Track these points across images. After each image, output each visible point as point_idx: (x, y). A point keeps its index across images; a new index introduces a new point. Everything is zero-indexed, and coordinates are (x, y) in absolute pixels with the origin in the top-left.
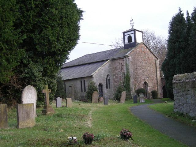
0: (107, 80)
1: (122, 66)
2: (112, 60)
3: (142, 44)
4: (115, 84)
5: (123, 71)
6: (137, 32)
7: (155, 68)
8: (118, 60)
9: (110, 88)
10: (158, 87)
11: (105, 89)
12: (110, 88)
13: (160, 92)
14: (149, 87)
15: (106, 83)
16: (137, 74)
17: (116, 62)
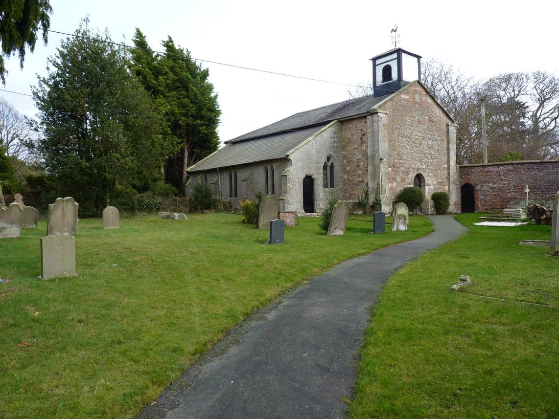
0: (325, 167)
1: (363, 135)
2: (342, 122)
3: (417, 84)
4: (346, 177)
5: (364, 146)
6: (404, 55)
7: (446, 142)
8: (355, 122)
9: (332, 186)
10: (449, 186)
12: (332, 186)
13: (454, 198)
14: (427, 187)
17: (350, 125)
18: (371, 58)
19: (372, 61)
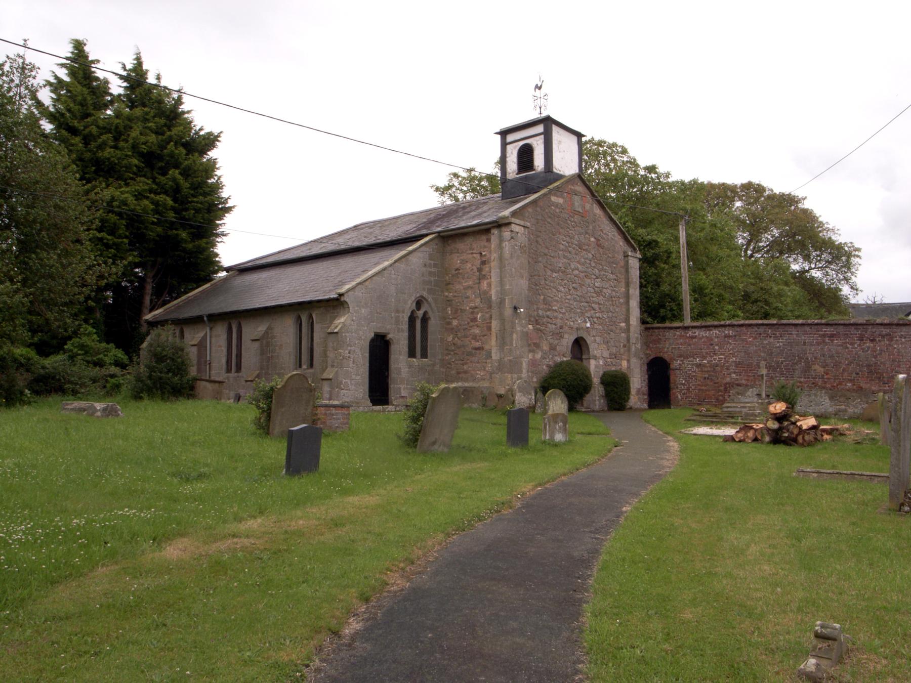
0: (412, 319)
1: (483, 263)
2: (448, 238)
3: (578, 180)
4: (450, 339)
5: (485, 284)
6: (555, 129)
7: (623, 284)
8: (469, 240)
9: (424, 355)
10: (628, 361)
11: (401, 363)
12: (424, 355)
13: (638, 382)
14: (593, 363)
15: (406, 334)
16: (545, 302)
17: (461, 245)
18: (498, 130)
19: (499, 136)
